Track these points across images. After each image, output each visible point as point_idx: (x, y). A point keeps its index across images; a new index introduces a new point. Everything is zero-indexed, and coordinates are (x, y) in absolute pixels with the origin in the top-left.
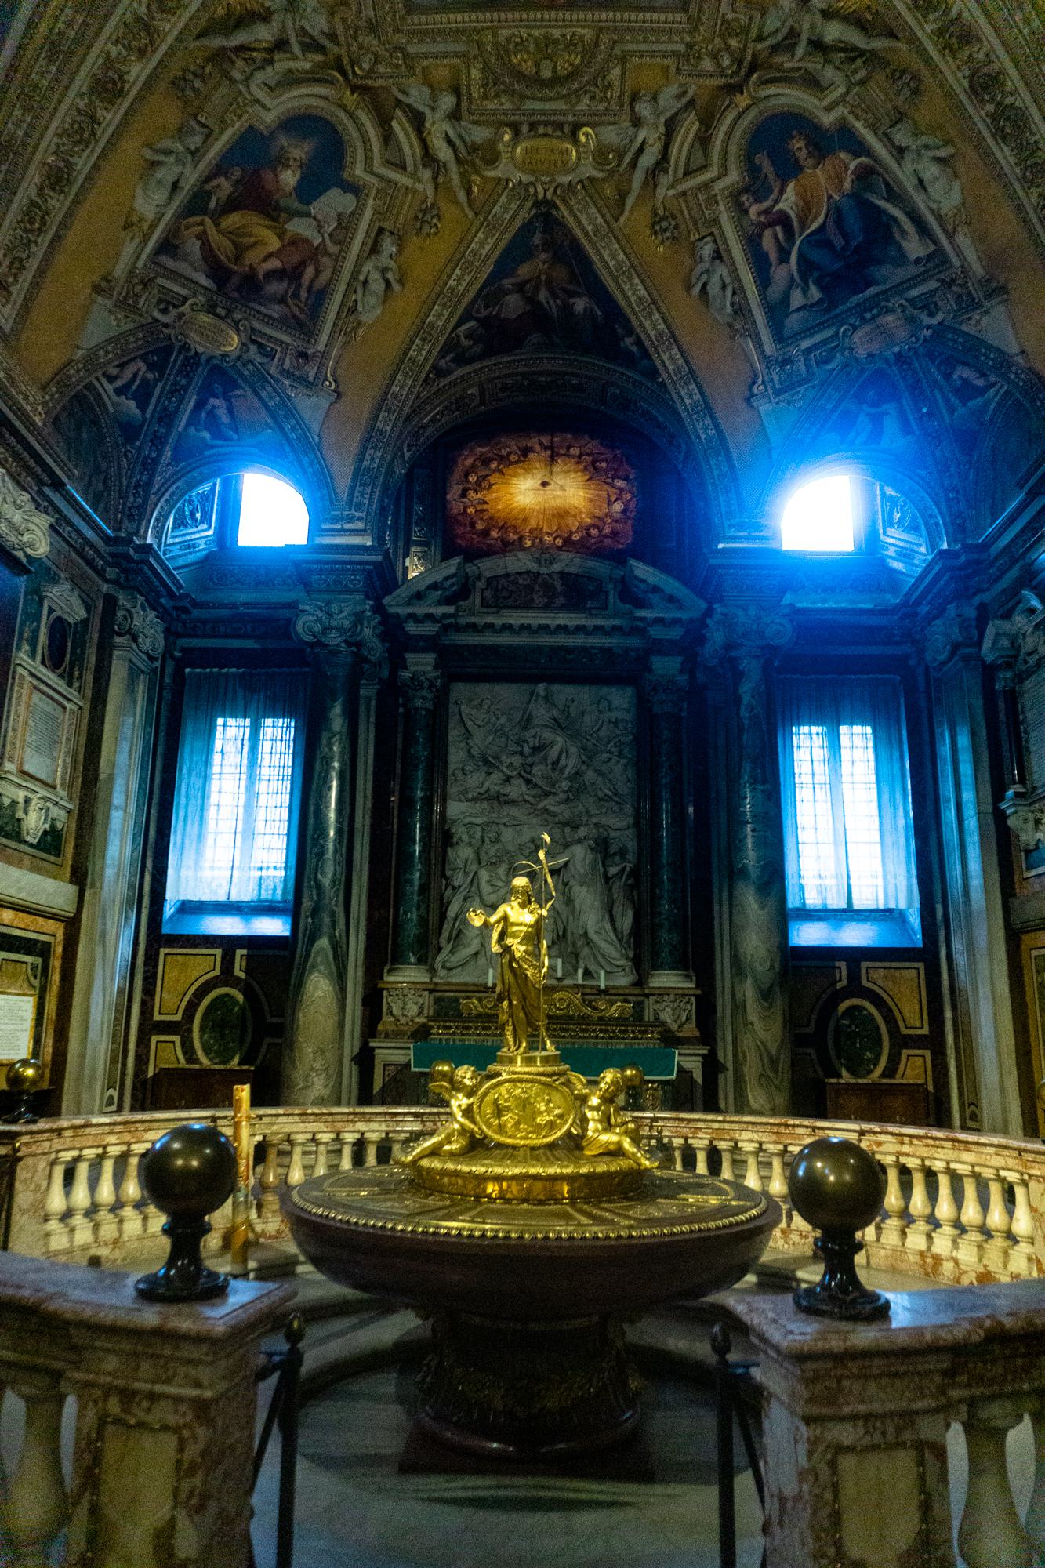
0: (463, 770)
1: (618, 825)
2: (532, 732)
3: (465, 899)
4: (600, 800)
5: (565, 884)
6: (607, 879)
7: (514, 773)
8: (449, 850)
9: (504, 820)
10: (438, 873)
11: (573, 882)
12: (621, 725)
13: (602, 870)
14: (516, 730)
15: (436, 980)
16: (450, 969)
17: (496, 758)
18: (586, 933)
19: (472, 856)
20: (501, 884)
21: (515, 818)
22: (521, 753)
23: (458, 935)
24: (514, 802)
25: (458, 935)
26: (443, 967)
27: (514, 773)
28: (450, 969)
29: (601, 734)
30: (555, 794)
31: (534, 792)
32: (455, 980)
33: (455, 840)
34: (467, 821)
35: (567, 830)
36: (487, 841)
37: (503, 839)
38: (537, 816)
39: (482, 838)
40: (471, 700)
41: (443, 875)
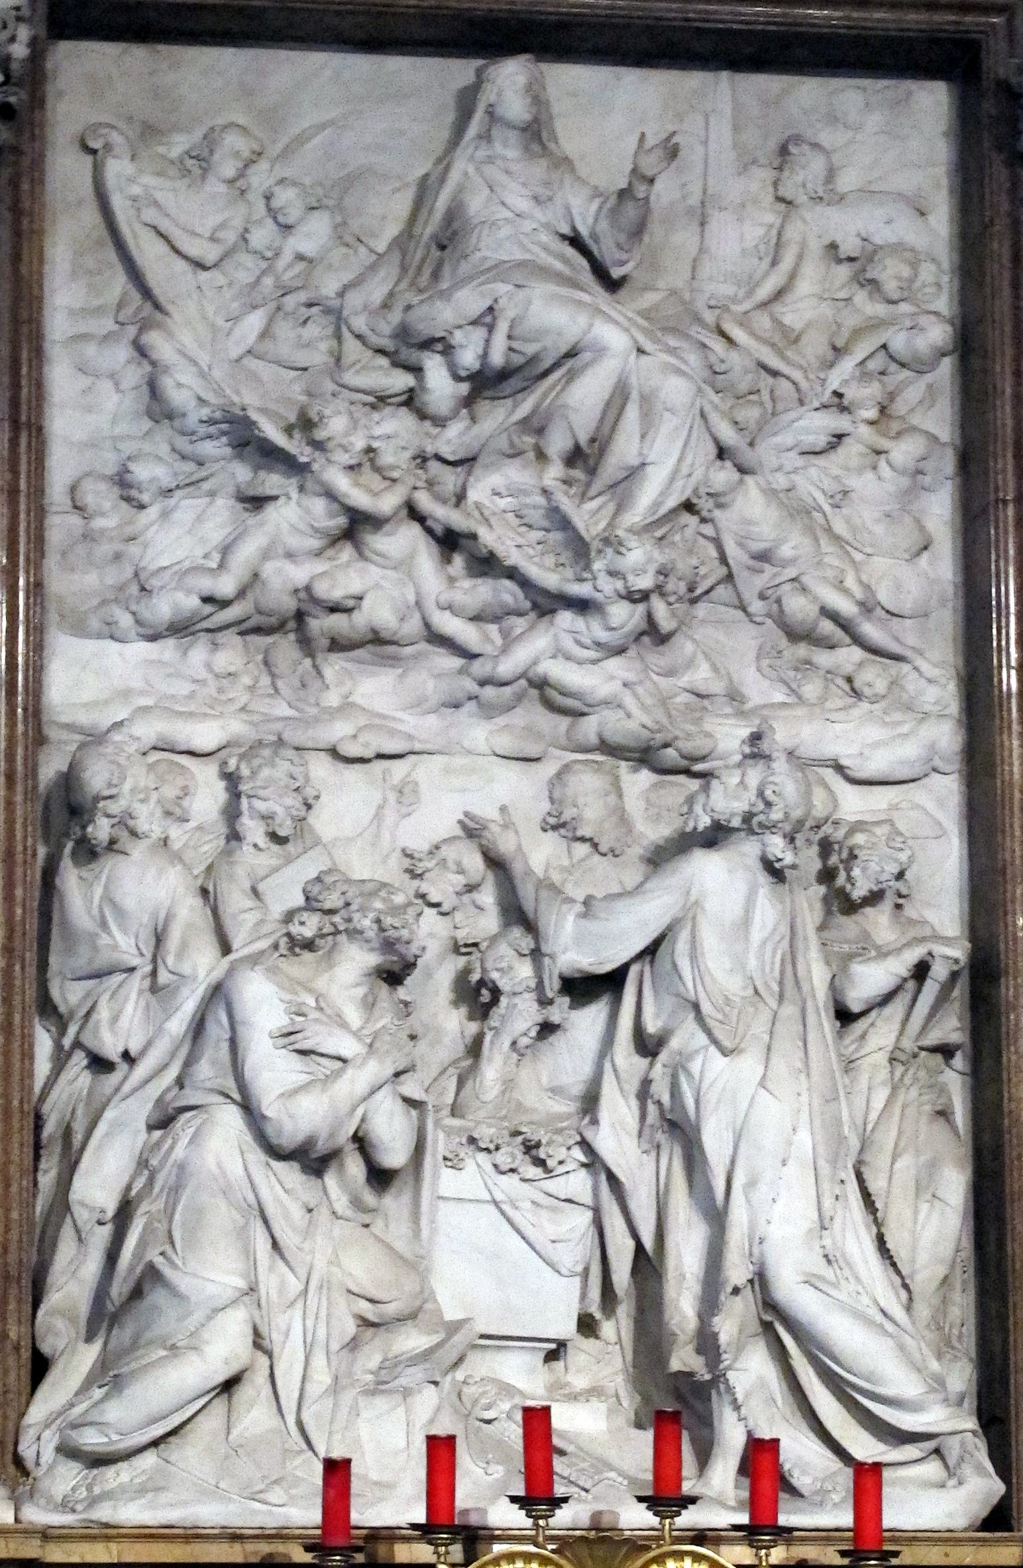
0: (123, 482)
1: (875, 766)
2: (471, 301)
3: (164, 1121)
4: (796, 634)
5: (647, 1046)
6: (845, 1016)
7: (388, 503)
8: (70, 878)
9: (338, 731)
10: (31, 993)
11: (687, 1036)
12: (890, 273)
13: (818, 975)
14: (376, 291)
15: (35, 1515)
16: (99, 1461)
17: (306, 424)
18: (760, 1280)
19: (189, 910)
20: (347, 1046)
21: (378, 722)
22: (411, 400)
23: (137, 1293)
24: (377, 639)
25: (137, 1293)
26: (68, 1451)
27: (388, 503)
28: (99, 1461)
29: (794, 314)
30: (582, 606)
31: (482, 592)
32: (132, 1513)
33: (101, 830)
34: (148, 730)
35: (637, 782)
36: (254, 831)
37: (323, 822)
38: (489, 711)
39: (231, 813)
40: (150, 132)
41: (47, 1007)
